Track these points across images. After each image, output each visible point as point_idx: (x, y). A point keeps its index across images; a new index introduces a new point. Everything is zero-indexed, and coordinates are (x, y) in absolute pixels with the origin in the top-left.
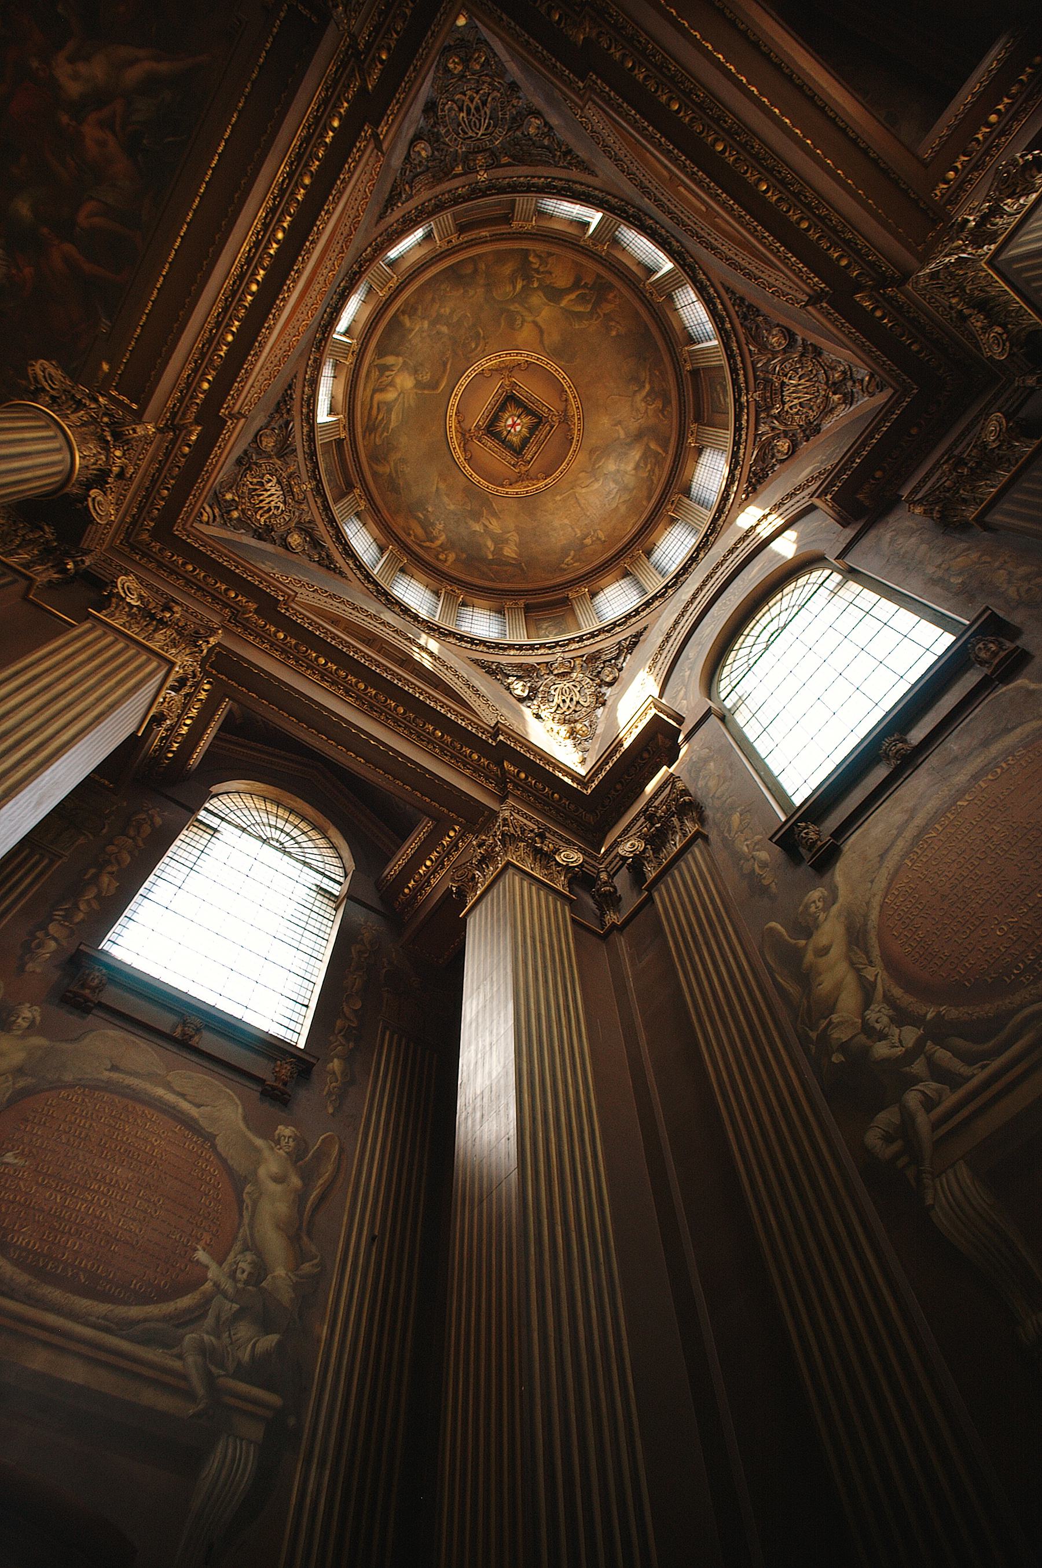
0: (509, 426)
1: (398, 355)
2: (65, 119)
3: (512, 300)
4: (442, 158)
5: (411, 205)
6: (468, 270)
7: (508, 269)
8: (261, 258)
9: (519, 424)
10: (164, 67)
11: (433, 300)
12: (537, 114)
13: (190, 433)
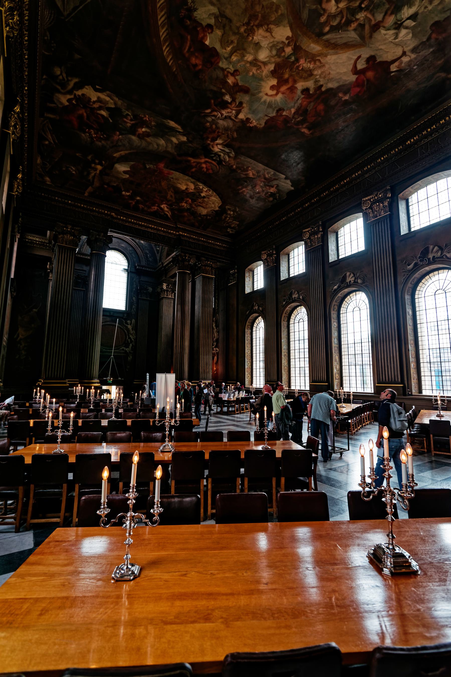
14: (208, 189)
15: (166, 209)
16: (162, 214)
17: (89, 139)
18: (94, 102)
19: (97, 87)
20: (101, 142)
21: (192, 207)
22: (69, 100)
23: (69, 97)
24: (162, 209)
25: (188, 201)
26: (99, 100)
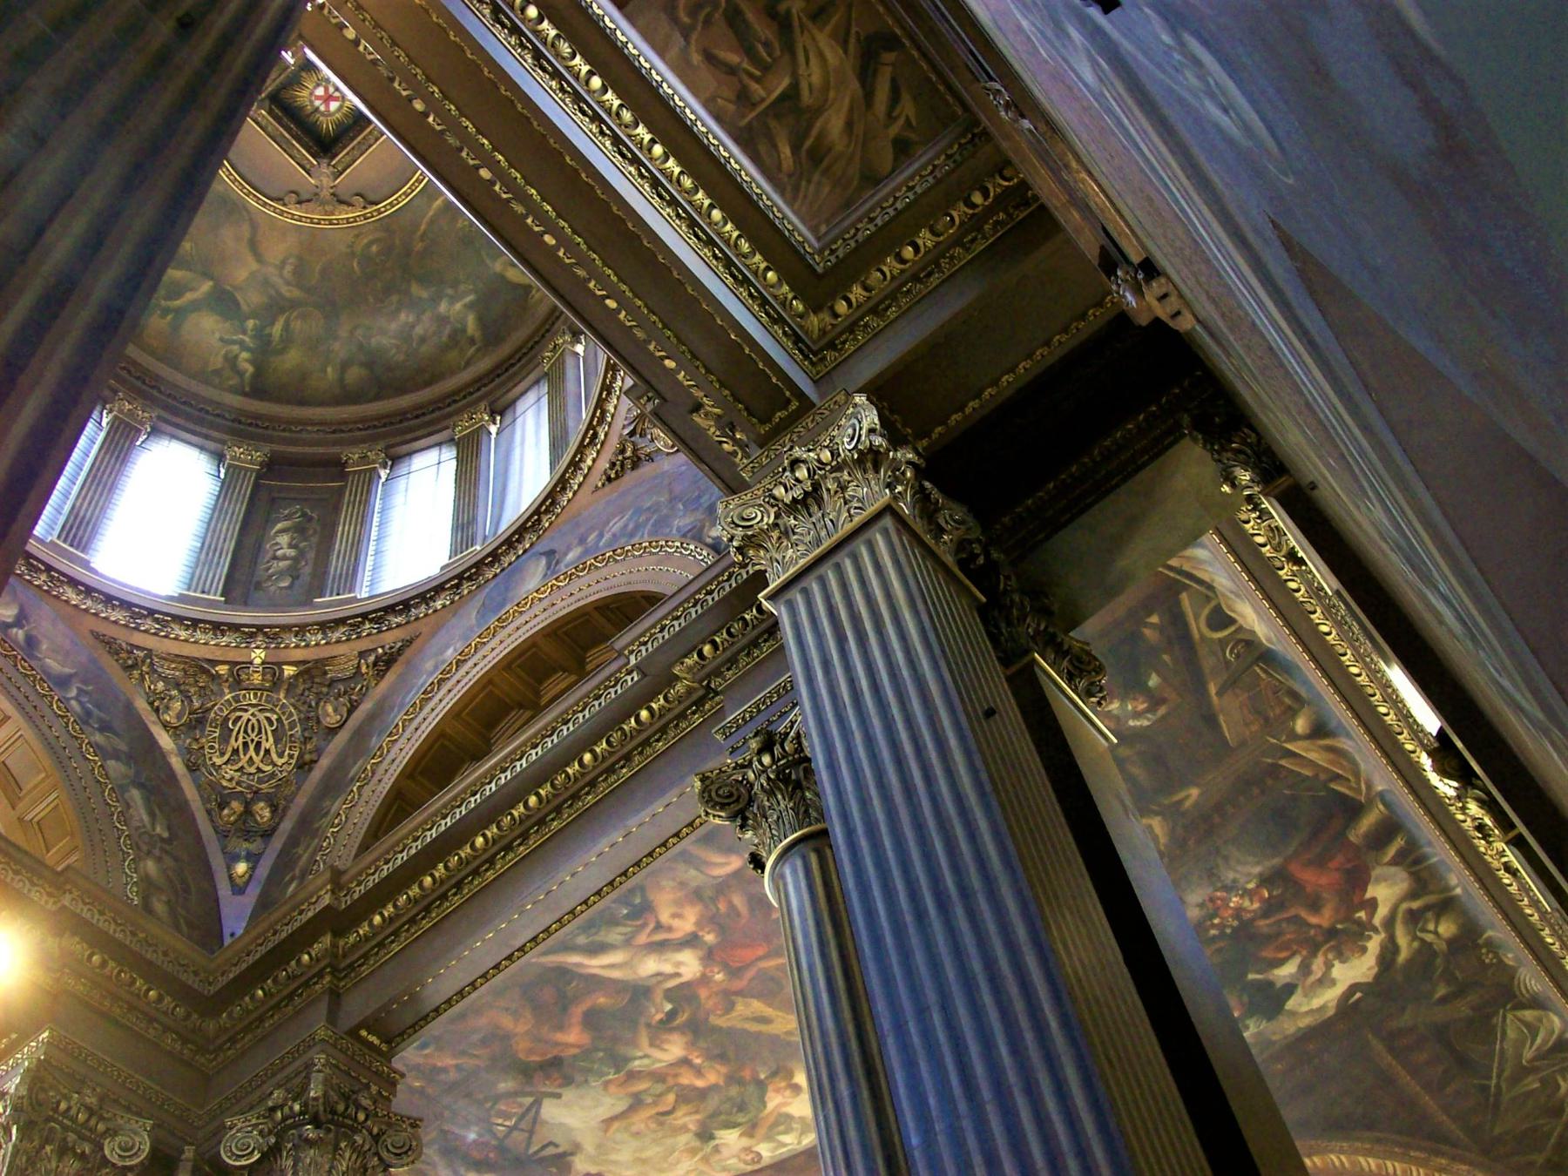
0: (336, 99)
1: (502, 278)
2: (710, 938)
3: (294, 304)
4: (307, 693)
5: (364, 645)
6: (355, 374)
7: (292, 358)
8: (511, 828)
9: (318, 98)
10: (574, 959)
11: (423, 340)
12: (166, 726)
13: (690, 669)
14: (764, 1163)
15: (650, 966)
16: (614, 935)
17: (1231, 875)
18: (1329, 966)
19: (1358, 995)
20: (1201, 905)
21: (633, 1076)
22: (1372, 905)
23: (1382, 911)
24: (660, 947)
25: (699, 1072)
26: (1326, 981)
